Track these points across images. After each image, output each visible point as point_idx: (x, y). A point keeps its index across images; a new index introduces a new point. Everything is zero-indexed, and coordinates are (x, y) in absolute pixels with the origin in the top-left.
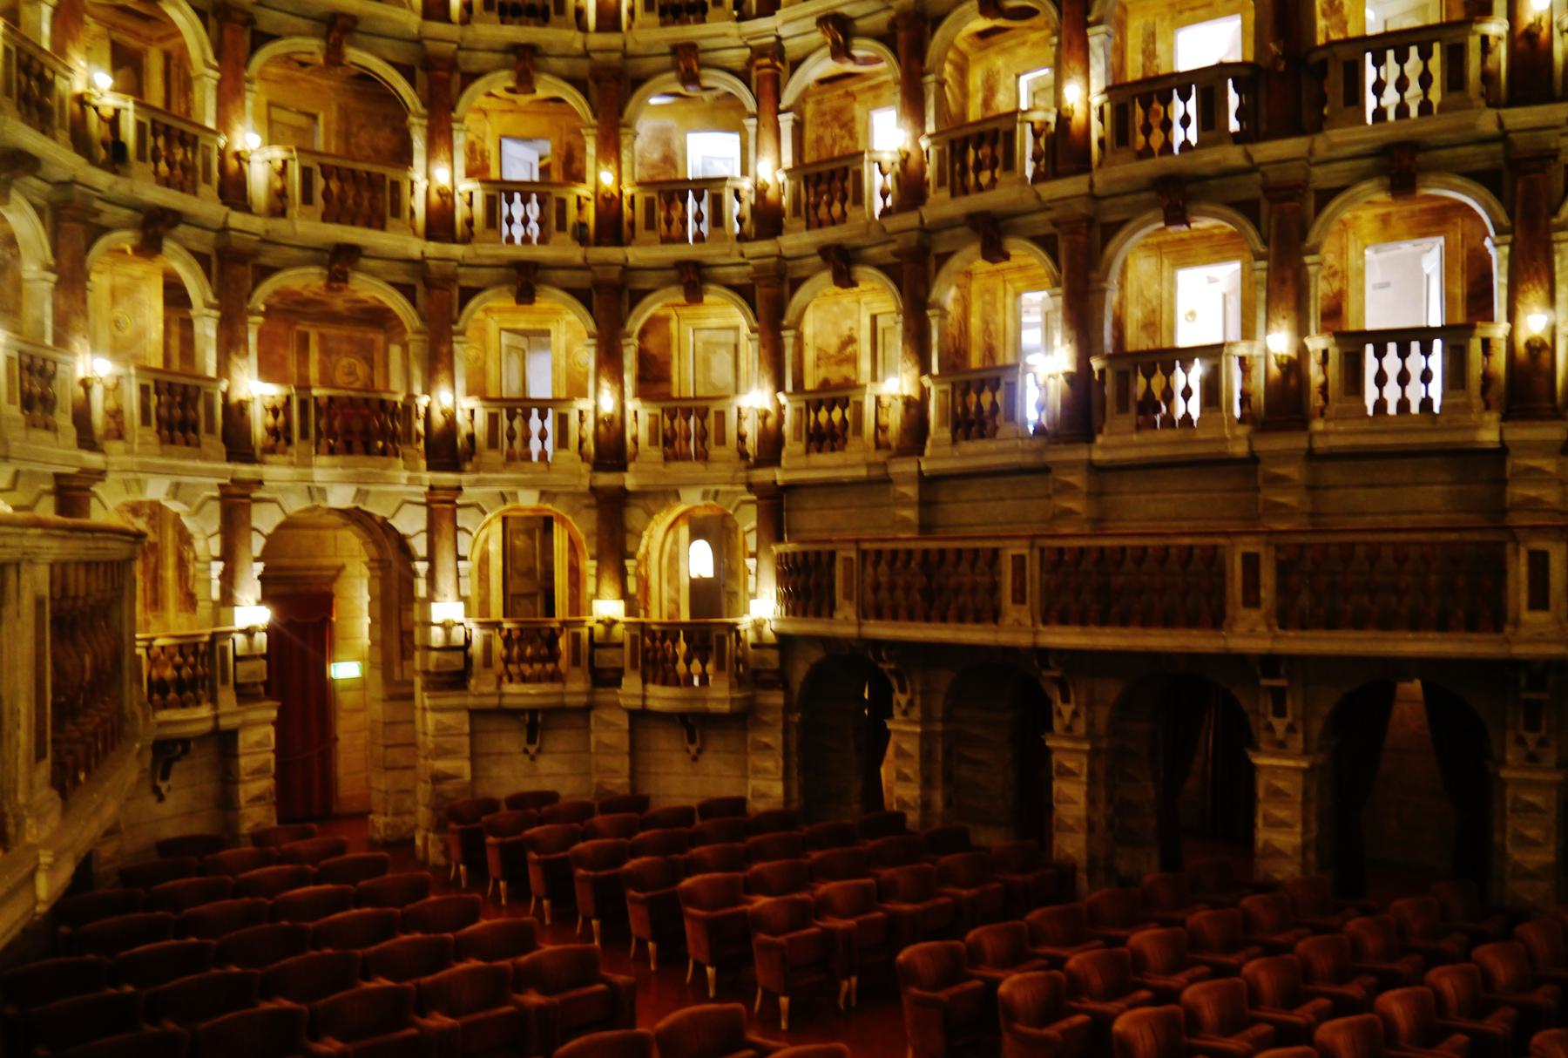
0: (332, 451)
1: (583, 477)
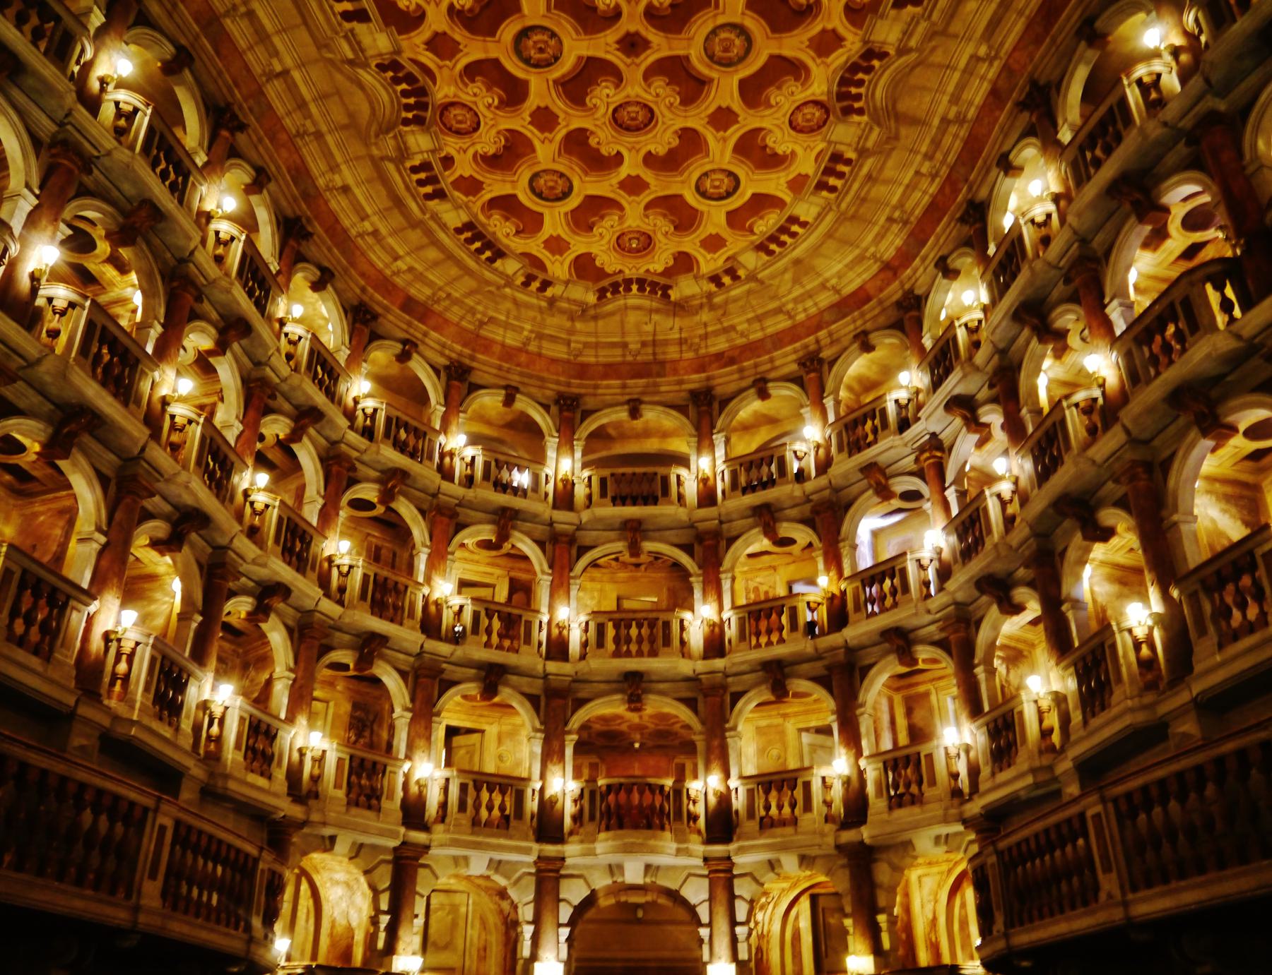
0: (608, 829)
1: (831, 837)
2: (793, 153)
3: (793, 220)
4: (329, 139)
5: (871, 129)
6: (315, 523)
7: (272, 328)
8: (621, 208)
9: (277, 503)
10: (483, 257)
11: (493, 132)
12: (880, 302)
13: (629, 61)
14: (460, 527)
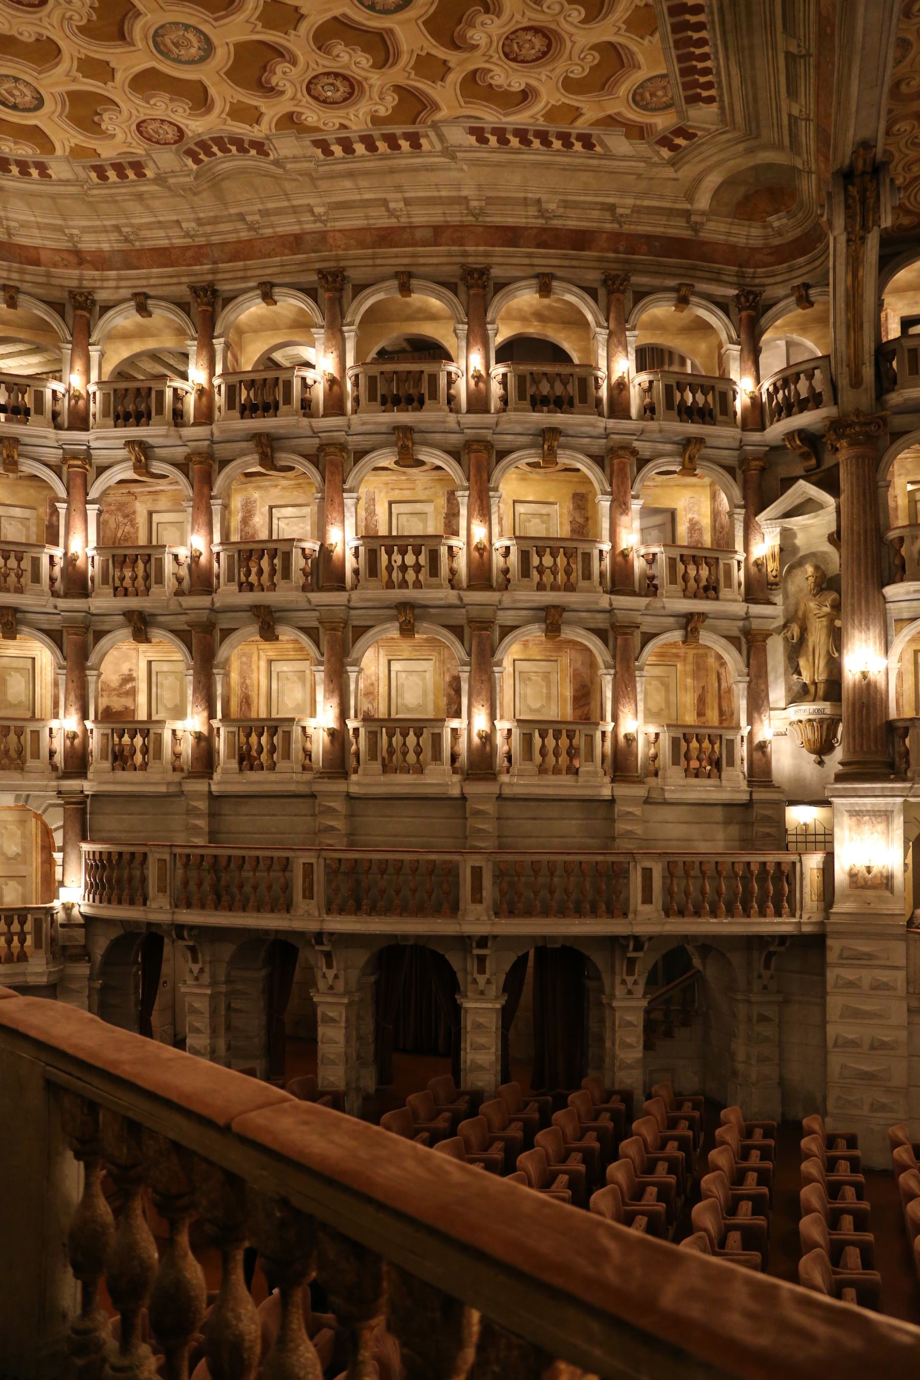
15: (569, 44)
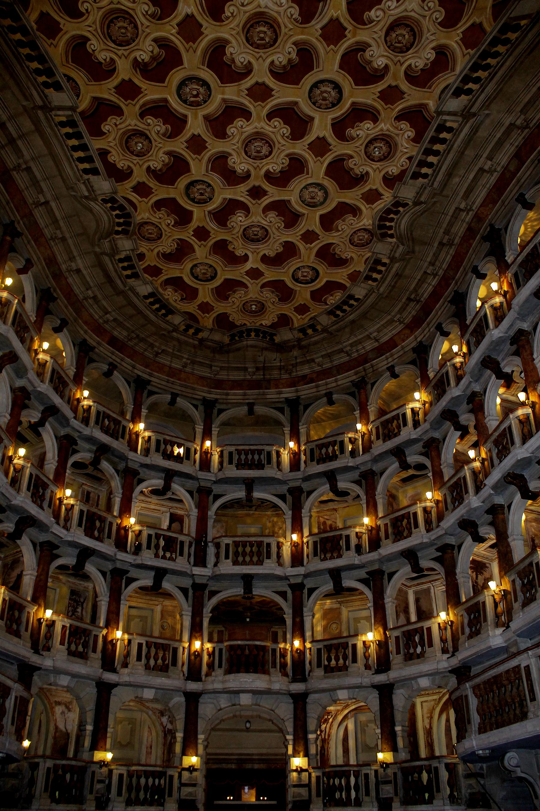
2: (352, 258)
3: (351, 297)
4: (70, 241)
5: (398, 246)
6: (51, 477)
7: (31, 356)
8: (246, 286)
9: (29, 465)
10: (160, 313)
11: (171, 239)
12: (403, 348)
13: (254, 202)
14: (141, 481)
15: (412, 14)
